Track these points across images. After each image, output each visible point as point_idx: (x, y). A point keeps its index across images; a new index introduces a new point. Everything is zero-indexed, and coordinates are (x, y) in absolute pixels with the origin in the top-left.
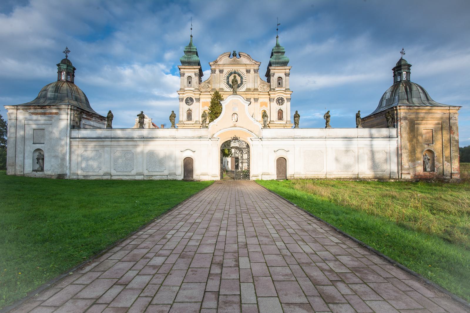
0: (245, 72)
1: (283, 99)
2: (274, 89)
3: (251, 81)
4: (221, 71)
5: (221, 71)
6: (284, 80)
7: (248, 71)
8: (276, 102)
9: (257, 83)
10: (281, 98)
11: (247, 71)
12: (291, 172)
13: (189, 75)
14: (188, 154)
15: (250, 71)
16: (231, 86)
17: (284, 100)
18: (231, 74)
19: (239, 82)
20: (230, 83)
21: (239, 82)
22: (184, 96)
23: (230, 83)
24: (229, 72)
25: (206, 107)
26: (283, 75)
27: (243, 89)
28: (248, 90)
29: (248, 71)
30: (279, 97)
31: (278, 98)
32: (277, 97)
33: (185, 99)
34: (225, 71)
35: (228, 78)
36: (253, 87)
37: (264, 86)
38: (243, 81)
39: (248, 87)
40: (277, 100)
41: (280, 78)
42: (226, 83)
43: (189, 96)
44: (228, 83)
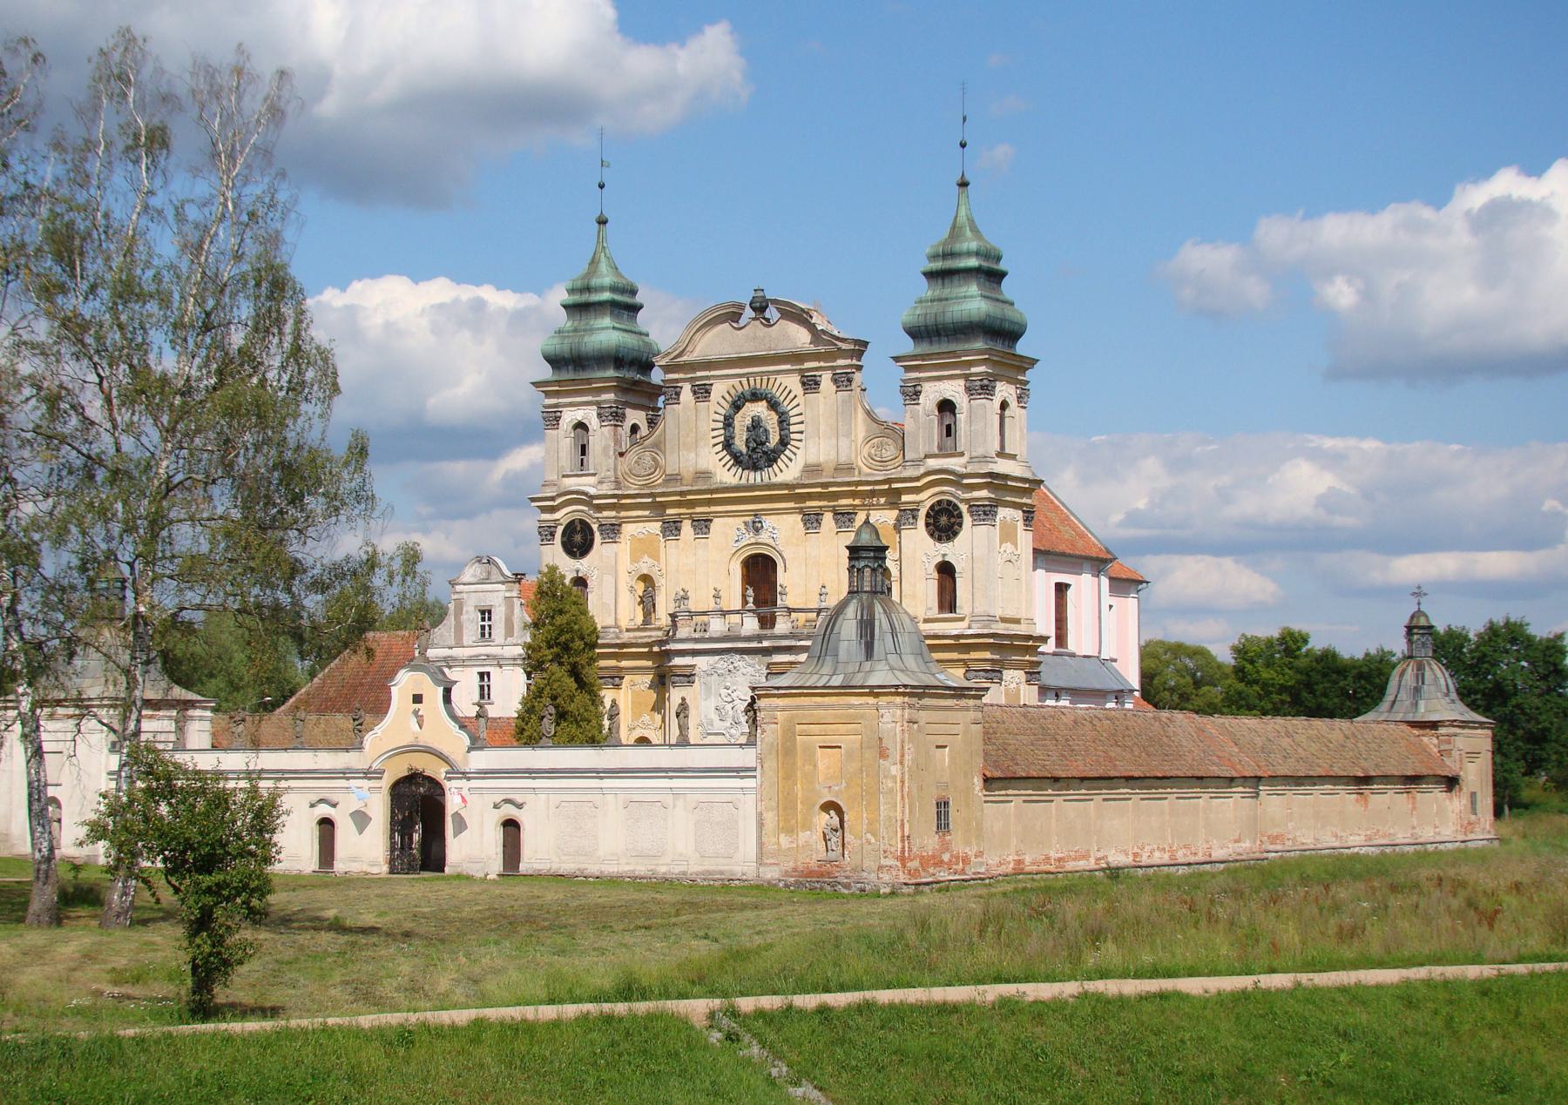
0: (798, 389)
1: (956, 507)
2: (918, 462)
3: (822, 428)
4: (702, 392)
5: (702, 392)
6: (962, 417)
7: (810, 384)
8: (927, 525)
9: (848, 434)
10: (949, 503)
11: (803, 384)
12: (534, 856)
13: (579, 414)
14: (324, 810)
15: (817, 384)
16: (737, 459)
17: (960, 516)
18: (737, 406)
19: (774, 439)
20: (740, 444)
21: (774, 439)
22: (557, 516)
23: (740, 444)
24: (733, 392)
25: (646, 558)
26: (953, 389)
27: (787, 471)
28: (812, 469)
29: (810, 384)
30: (939, 502)
31: (932, 507)
32: (928, 504)
33: (560, 530)
34: (721, 390)
35: (728, 423)
36: (833, 456)
37: (881, 446)
38: (792, 428)
39: (812, 459)
40: (928, 515)
41: (946, 407)
42: (720, 447)
43: (578, 516)
44: (728, 445)
